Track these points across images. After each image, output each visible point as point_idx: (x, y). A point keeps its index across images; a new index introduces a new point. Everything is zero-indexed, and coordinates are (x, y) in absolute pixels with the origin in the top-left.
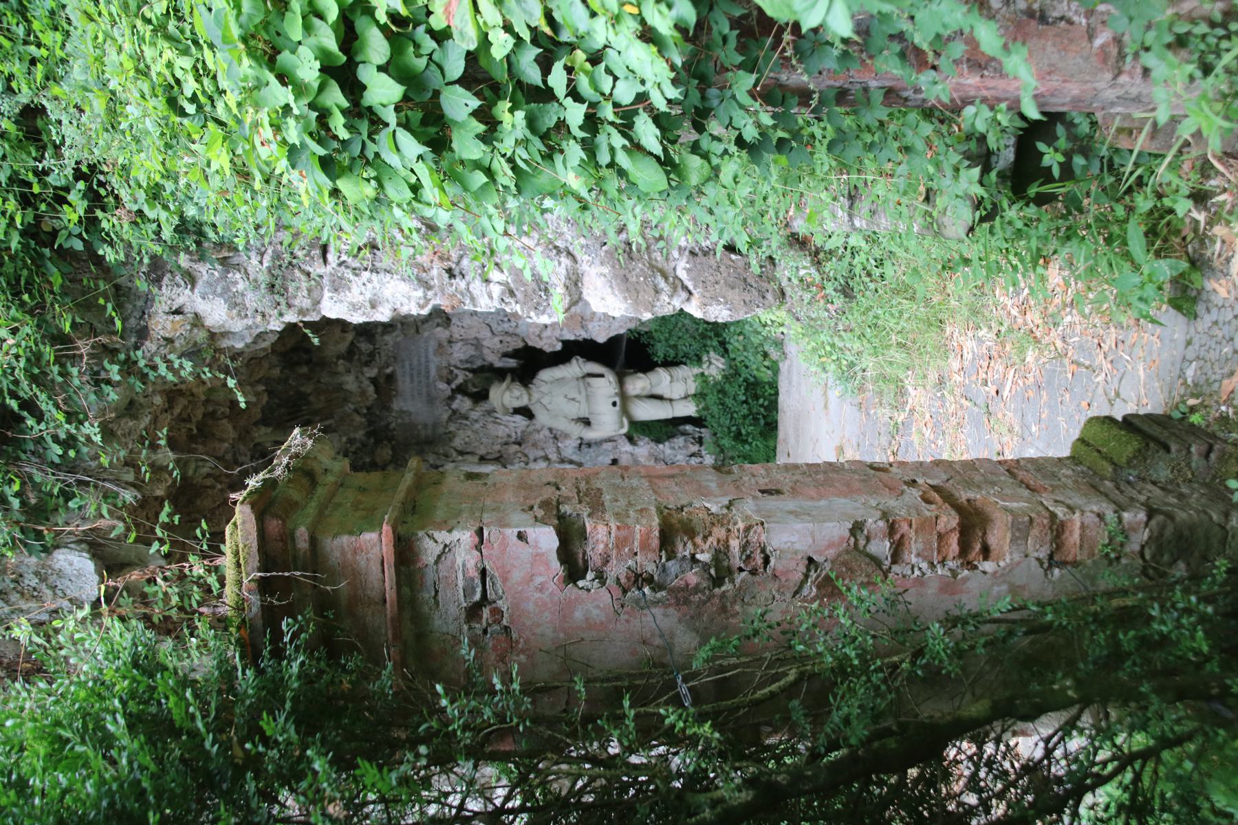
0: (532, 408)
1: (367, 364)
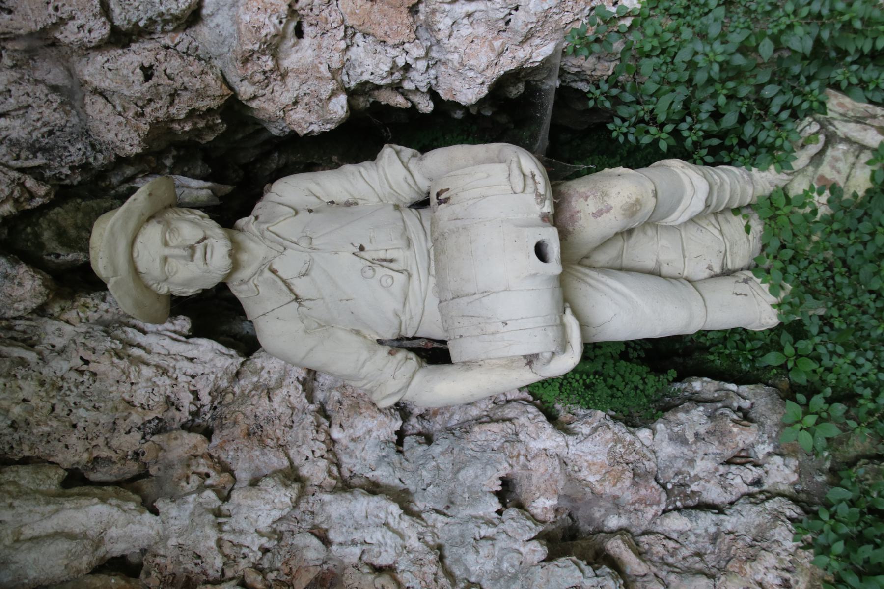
0: (239, 291)
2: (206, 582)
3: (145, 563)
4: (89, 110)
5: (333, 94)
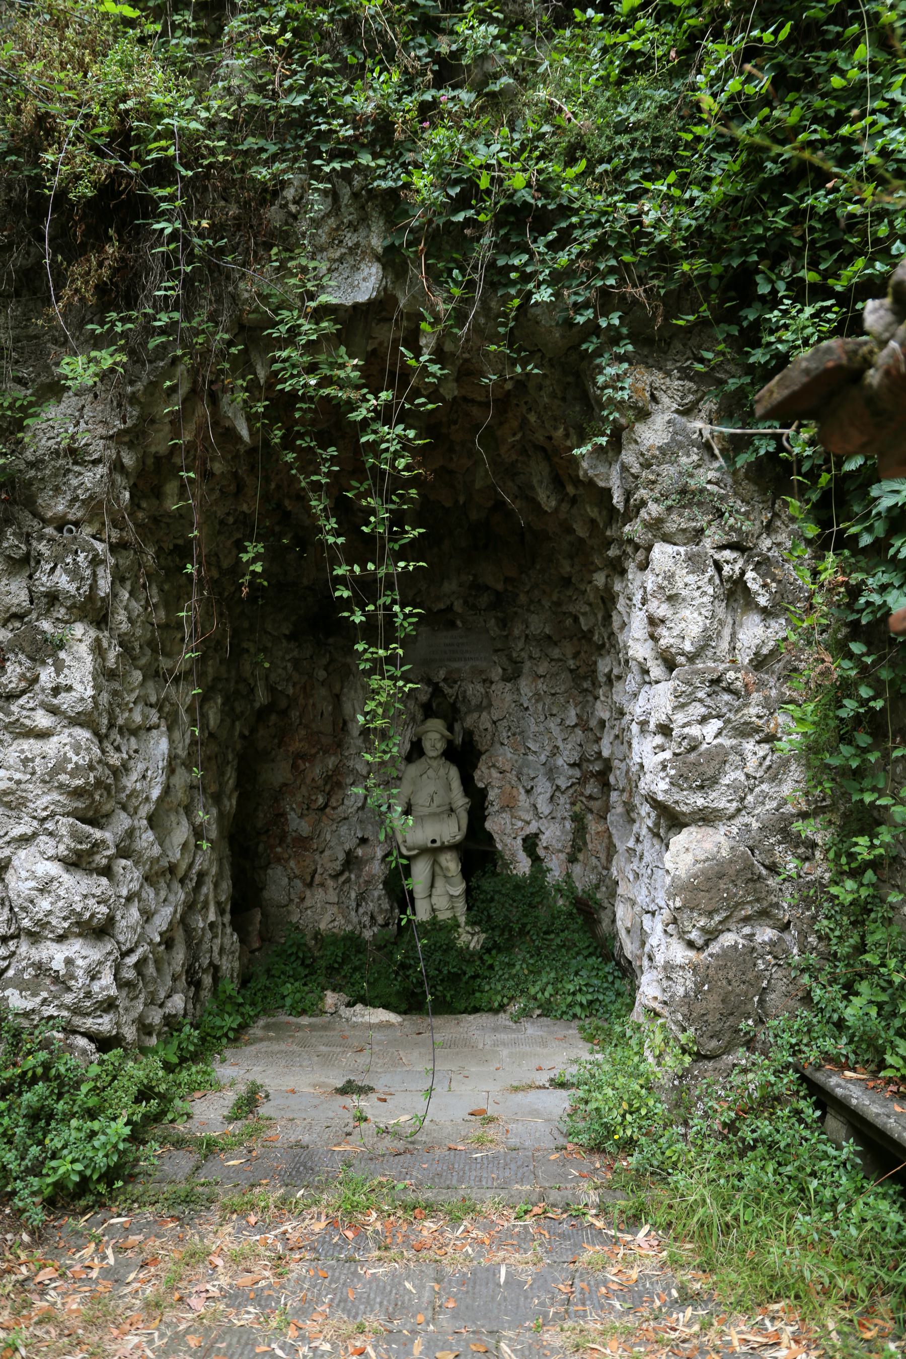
1: (466, 602)
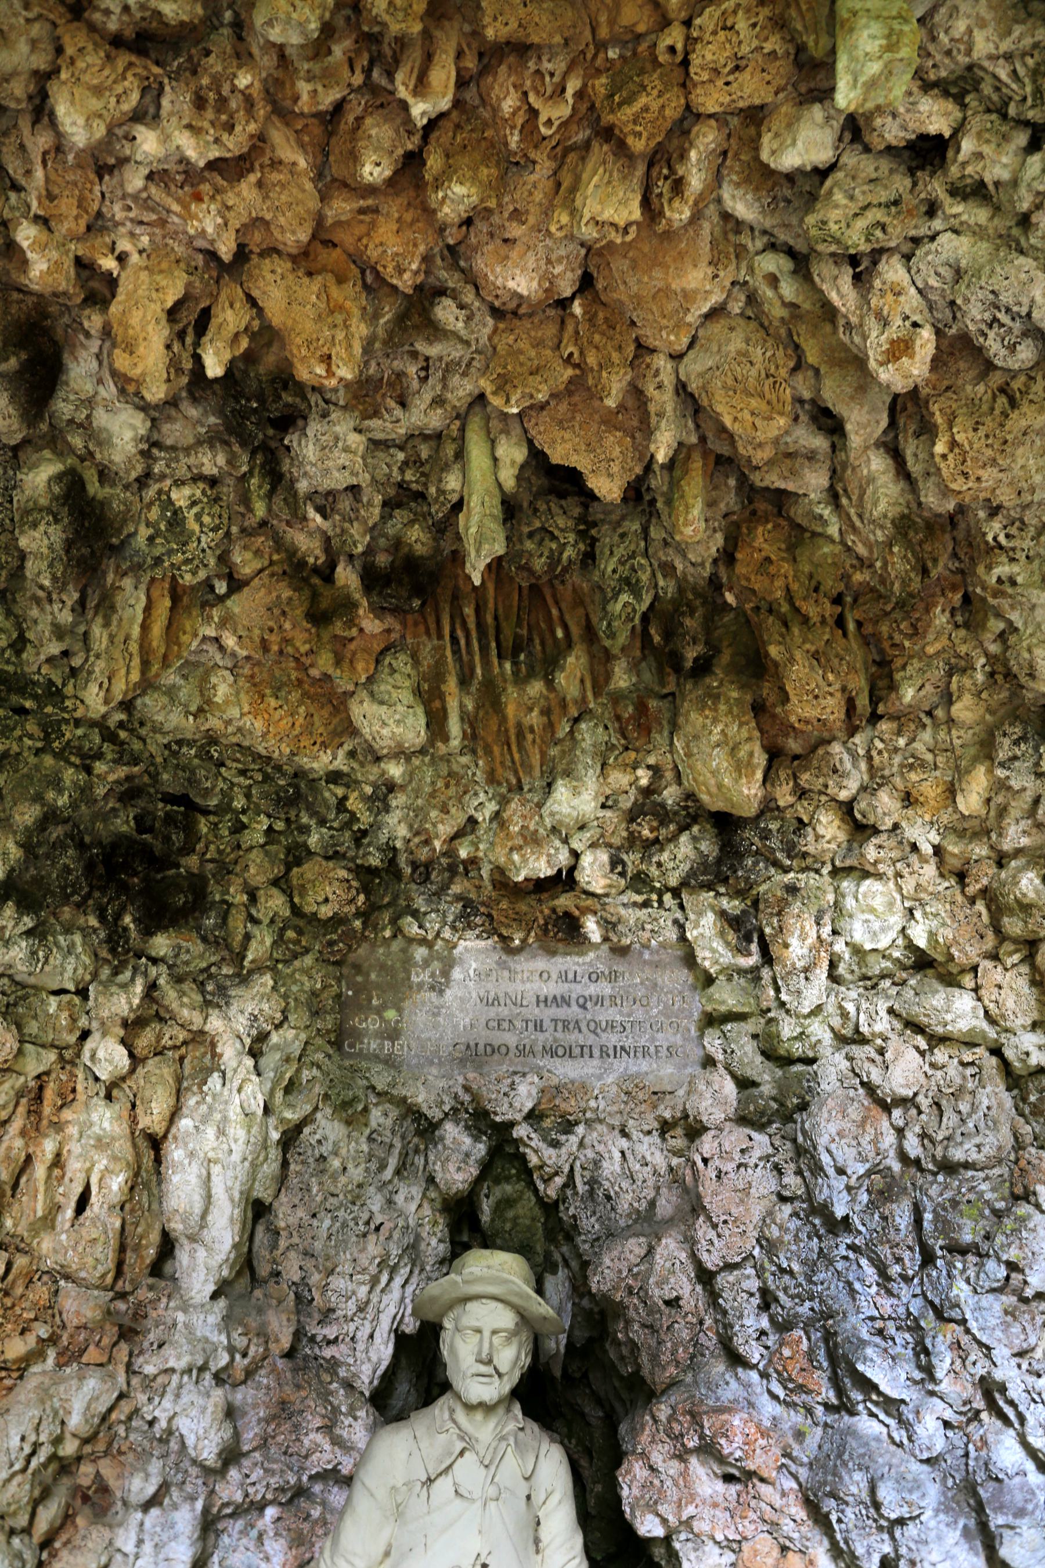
1: (615, 862)
2: (131, 1355)
3: (163, 1284)
4: (632, 1241)
5: (664, 1521)
